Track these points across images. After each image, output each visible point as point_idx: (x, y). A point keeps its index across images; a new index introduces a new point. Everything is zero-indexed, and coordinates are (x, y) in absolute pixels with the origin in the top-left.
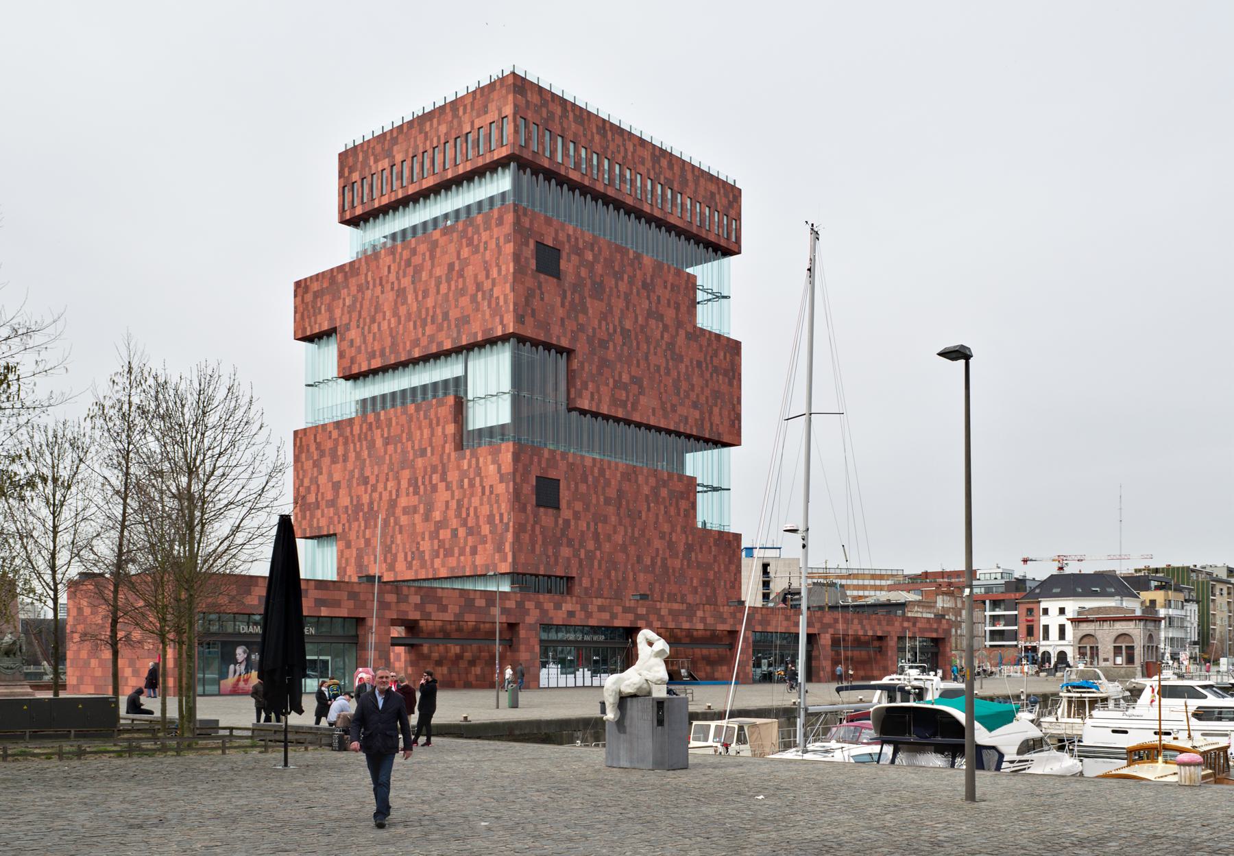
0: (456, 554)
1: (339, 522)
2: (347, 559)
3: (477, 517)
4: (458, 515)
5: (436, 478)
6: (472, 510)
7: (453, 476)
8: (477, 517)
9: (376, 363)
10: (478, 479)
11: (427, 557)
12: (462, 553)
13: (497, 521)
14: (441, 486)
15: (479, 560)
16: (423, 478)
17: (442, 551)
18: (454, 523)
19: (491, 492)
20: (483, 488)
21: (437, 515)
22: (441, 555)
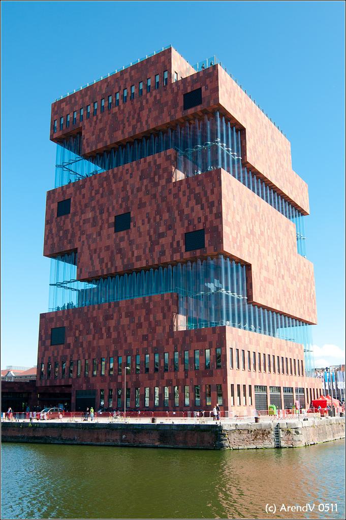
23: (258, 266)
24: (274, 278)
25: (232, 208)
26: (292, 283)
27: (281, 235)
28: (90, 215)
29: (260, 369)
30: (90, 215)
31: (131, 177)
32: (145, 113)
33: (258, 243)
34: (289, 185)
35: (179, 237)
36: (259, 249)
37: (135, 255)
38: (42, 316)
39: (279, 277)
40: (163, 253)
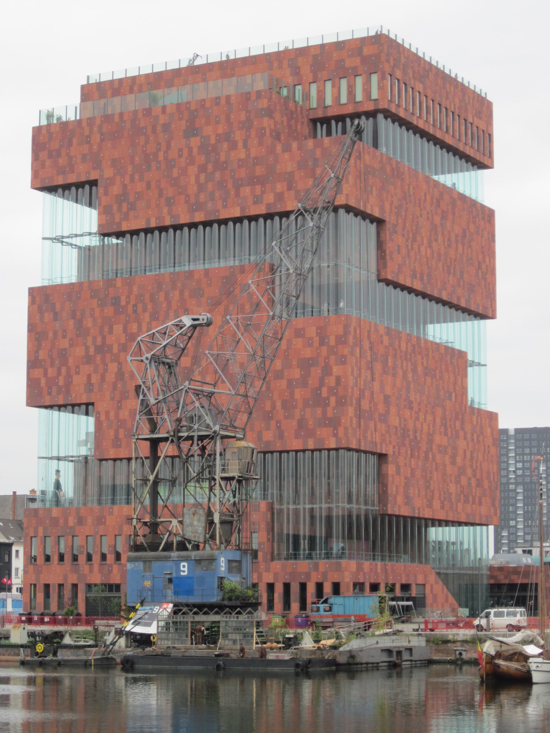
0: (471, 503)
1: (390, 443)
2: (397, 486)
3: (482, 471)
4: (471, 466)
5: (458, 424)
6: (479, 463)
7: (468, 427)
8: (482, 471)
9: (418, 286)
10: (481, 436)
11: (453, 501)
12: (474, 503)
13: (492, 480)
14: (461, 434)
15: (483, 510)
16: (450, 421)
17: (462, 496)
18: (469, 472)
19: (489, 451)
20: (485, 446)
21: (459, 460)
22: (462, 501)
23: (112, 399)
25: (51, 335)
34: (246, 191)
36: (120, 369)
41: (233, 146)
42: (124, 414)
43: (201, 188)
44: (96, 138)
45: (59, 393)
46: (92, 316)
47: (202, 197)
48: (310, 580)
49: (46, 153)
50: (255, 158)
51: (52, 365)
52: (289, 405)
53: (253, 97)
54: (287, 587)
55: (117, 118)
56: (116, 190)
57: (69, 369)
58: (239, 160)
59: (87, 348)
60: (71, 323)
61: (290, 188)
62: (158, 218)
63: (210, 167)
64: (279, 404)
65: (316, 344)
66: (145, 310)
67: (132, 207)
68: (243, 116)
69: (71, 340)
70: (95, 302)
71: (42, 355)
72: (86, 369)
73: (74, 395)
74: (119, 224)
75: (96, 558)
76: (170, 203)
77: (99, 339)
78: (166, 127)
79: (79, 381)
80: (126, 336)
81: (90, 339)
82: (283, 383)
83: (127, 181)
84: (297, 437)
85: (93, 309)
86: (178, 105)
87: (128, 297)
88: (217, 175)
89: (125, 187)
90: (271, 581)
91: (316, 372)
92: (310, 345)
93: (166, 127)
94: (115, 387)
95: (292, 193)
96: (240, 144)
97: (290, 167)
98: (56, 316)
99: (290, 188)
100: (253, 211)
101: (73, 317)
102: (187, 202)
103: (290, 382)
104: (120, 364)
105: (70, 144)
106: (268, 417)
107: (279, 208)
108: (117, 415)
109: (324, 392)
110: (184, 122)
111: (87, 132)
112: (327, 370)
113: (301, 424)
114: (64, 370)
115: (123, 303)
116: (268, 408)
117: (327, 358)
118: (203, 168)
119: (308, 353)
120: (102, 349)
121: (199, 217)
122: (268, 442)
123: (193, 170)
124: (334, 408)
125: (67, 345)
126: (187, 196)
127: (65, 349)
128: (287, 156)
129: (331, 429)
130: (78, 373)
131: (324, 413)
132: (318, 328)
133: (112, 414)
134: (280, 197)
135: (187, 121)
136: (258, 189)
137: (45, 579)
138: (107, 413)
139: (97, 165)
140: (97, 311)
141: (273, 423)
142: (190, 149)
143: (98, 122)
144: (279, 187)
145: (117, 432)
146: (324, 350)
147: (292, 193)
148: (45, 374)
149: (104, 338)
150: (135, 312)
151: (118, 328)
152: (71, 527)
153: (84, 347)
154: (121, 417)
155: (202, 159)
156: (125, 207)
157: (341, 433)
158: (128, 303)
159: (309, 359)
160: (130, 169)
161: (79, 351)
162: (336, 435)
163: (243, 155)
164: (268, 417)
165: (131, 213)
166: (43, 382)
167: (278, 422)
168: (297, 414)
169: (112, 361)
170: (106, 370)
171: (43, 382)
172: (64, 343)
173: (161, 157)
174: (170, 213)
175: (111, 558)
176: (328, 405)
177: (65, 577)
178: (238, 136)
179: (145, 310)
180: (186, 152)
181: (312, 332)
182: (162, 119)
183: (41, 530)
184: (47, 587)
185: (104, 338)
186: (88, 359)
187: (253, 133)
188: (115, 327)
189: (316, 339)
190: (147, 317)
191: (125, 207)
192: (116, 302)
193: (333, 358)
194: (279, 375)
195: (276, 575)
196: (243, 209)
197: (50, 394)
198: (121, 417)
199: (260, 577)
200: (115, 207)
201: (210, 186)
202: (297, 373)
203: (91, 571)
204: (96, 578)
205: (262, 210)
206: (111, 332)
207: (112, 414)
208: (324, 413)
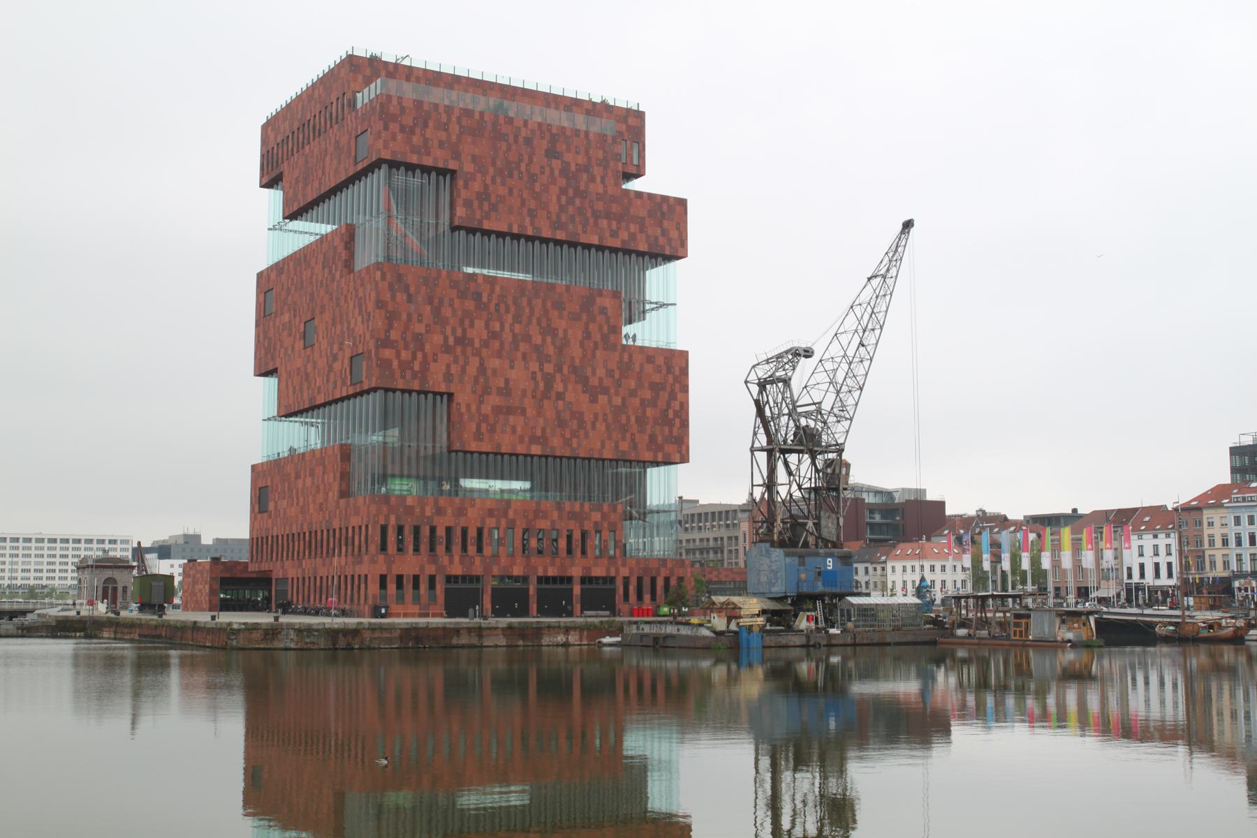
23: (474, 392)
24: (528, 402)
25: (404, 316)
26: (594, 400)
27: (561, 324)
28: (286, 317)
29: (464, 548)
30: (286, 317)
31: (316, 263)
32: (328, 158)
33: (478, 353)
34: (604, 223)
35: (347, 362)
36: (482, 364)
37: (317, 385)
38: (254, 468)
39: (545, 395)
40: (335, 382)
41: (592, 179)
42: (487, 409)
43: (562, 209)
44: (455, 128)
45: (414, 376)
46: (451, 305)
47: (564, 218)
48: (659, 575)
49: (397, 126)
50: (611, 196)
51: (406, 347)
52: (641, 421)
53: (610, 141)
54: (640, 580)
55: (477, 116)
56: (476, 186)
57: (425, 356)
58: (598, 194)
59: (446, 339)
60: (428, 308)
61: (641, 232)
62: (519, 226)
63: (571, 192)
64: (633, 419)
65: (664, 372)
66: (507, 311)
67: (494, 208)
68: (600, 154)
69: (427, 326)
70: (455, 291)
71: (394, 335)
72: (445, 358)
73: (431, 382)
74: (480, 222)
75: (456, 548)
76: (532, 214)
77: (459, 332)
78: (528, 141)
79: (433, 366)
80: (488, 332)
81: (449, 330)
82: (636, 402)
83: (489, 181)
84: (648, 450)
85: (452, 300)
86: (540, 125)
87: (490, 295)
88: (578, 201)
89: (486, 186)
90: (627, 575)
91: (664, 396)
92: (660, 372)
93: (528, 141)
94: (476, 381)
95: (644, 235)
96: (598, 179)
97: (643, 213)
98: (410, 299)
99: (641, 232)
100: (611, 242)
101: (431, 302)
102: (549, 218)
103: (642, 401)
104: (482, 359)
105: (426, 126)
106: (624, 429)
107: (632, 246)
108: (479, 409)
109: (671, 415)
110: (545, 142)
111: (444, 119)
112: (673, 396)
113: (652, 438)
114: (420, 355)
115: (485, 299)
116: (624, 421)
117: (673, 385)
118: (563, 191)
119: (657, 378)
120: (463, 341)
121: (561, 235)
122: (624, 452)
123: (554, 190)
124: (679, 429)
125: (423, 332)
126: (549, 212)
127: (421, 334)
128: (639, 202)
129: (676, 446)
130: (435, 361)
131: (671, 431)
132: (665, 358)
133: (474, 408)
134: (633, 237)
135: (548, 143)
136: (614, 224)
137: (396, 570)
138: (468, 406)
139: (457, 156)
140: (457, 302)
141: (628, 435)
142: (552, 170)
143: (457, 113)
144: (633, 228)
145: (478, 427)
146: (671, 379)
147: (644, 235)
148: (398, 355)
149: (464, 331)
150: (497, 311)
151: (480, 324)
152: (428, 517)
153: (442, 336)
154: (483, 412)
155: (562, 182)
156: (486, 206)
157: (684, 452)
158: (490, 301)
159: (659, 384)
160: (491, 170)
161: (437, 339)
162: (680, 452)
163: (601, 191)
164: (624, 429)
165: (493, 214)
166: (395, 364)
167: (633, 434)
168: (649, 429)
169: (473, 355)
170: (467, 363)
171: (395, 364)
172: (419, 328)
173: (523, 167)
174: (532, 224)
175: (472, 549)
176: (674, 425)
177: (422, 568)
178: (597, 171)
179: (507, 311)
180: (547, 170)
181: (660, 361)
182: (524, 133)
183: (393, 519)
184: (400, 579)
185: (464, 331)
186: (447, 349)
187: (610, 174)
188: (477, 322)
189: (664, 368)
190: (509, 318)
191: (486, 205)
192: (477, 297)
193: (677, 386)
194: (633, 393)
195: (631, 570)
196: (601, 239)
197: (403, 377)
198: (483, 412)
199: (617, 571)
200: (476, 204)
201: (571, 209)
202: (648, 394)
203: (451, 562)
204: (457, 570)
205: (617, 243)
206: (472, 325)
207: (474, 408)
208: (671, 431)
